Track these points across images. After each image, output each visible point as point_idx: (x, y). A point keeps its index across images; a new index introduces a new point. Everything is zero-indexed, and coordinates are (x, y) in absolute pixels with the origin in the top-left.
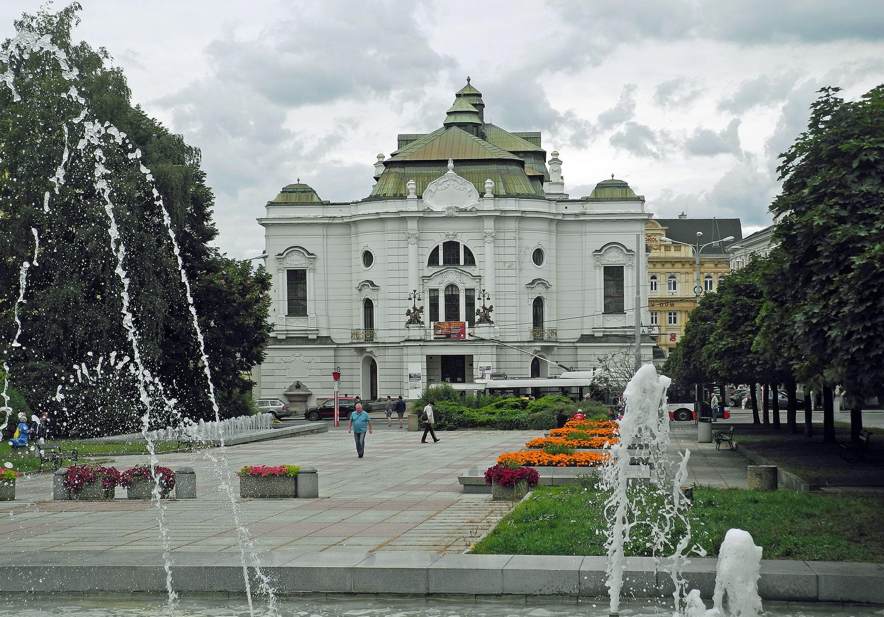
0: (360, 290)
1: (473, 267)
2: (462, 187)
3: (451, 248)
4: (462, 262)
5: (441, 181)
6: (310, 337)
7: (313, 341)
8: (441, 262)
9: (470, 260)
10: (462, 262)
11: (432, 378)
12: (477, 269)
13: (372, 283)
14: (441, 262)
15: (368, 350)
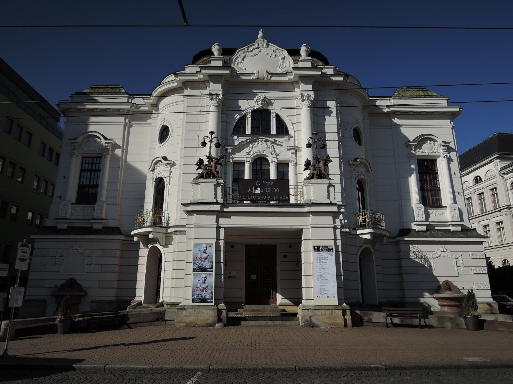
0: (153, 170)
1: (286, 138)
2: (274, 54)
3: (261, 117)
4: (273, 131)
5: (250, 49)
6: (96, 226)
7: (97, 232)
8: (248, 131)
9: (282, 129)
10: (273, 131)
11: (233, 273)
12: (292, 140)
13: (165, 159)
14: (248, 131)
15: (151, 236)
